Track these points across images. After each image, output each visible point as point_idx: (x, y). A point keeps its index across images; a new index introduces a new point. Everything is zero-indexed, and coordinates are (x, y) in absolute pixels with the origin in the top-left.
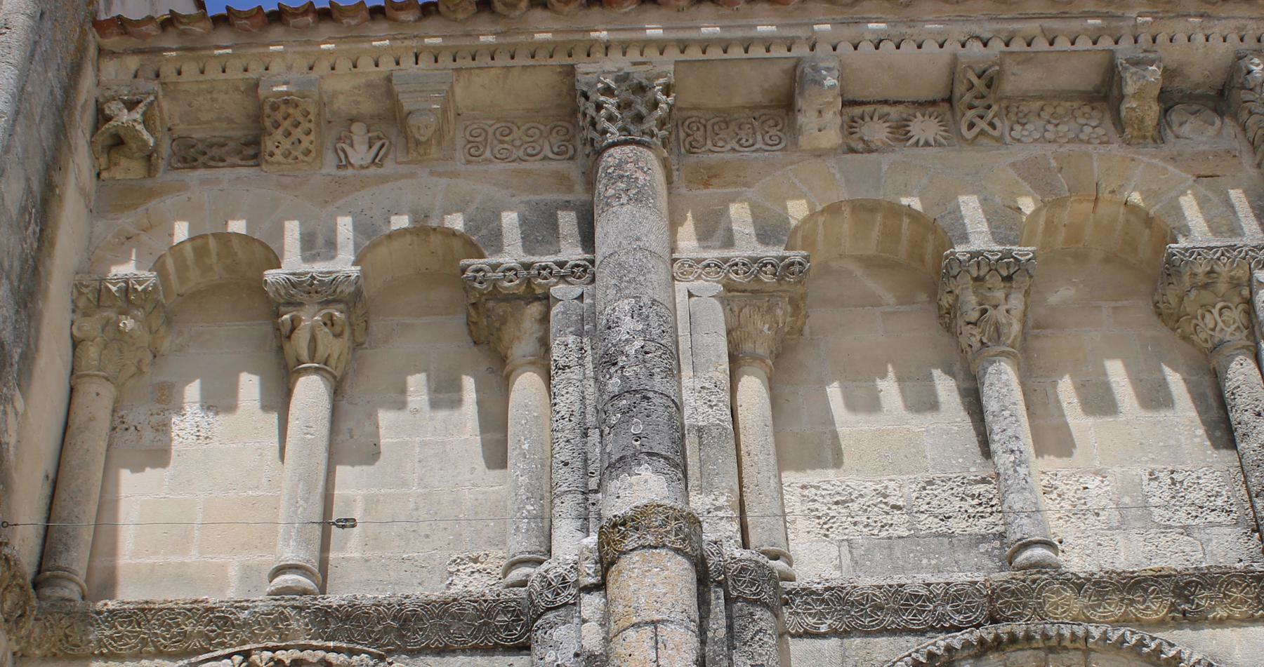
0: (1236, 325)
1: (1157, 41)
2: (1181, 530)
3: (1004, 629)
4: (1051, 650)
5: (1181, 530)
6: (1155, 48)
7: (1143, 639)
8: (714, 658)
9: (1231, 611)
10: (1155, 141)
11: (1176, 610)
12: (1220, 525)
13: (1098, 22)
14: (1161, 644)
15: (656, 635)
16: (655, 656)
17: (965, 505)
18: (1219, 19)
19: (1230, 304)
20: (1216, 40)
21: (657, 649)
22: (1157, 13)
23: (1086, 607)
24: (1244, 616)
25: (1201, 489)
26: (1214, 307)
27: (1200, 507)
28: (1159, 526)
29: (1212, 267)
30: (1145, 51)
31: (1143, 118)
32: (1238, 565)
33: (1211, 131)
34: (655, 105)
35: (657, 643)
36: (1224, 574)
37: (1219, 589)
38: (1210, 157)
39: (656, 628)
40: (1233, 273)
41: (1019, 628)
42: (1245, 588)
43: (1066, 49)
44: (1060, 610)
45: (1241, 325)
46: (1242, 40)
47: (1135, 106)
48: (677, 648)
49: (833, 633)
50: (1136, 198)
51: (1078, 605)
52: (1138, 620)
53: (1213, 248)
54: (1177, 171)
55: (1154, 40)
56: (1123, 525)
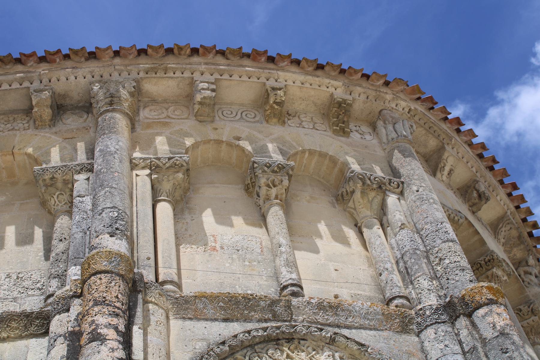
0: (65, 202)
1: (51, 81)
2: (12, 300)
5: (12, 300)
6: (50, 84)
9: (9, 333)
10: (50, 126)
12: (33, 295)
13: (22, 75)
18: (81, 68)
19: (63, 193)
20: (81, 79)
22: (52, 68)
24: (17, 335)
25: (31, 280)
26: (55, 195)
27: (27, 288)
29: (53, 176)
30: (45, 86)
31: (41, 116)
33: (81, 120)
36: (10, 315)
37: (5, 323)
38: (74, 131)
40: (64, 178)
42: (19, 321)
43: (7, 88)
45: (68, 202)
46: (93, 77)
47: (36, 110)
50: (30, 150)
53: (55, 167)
54: (56, 138)
55: (50, 81)
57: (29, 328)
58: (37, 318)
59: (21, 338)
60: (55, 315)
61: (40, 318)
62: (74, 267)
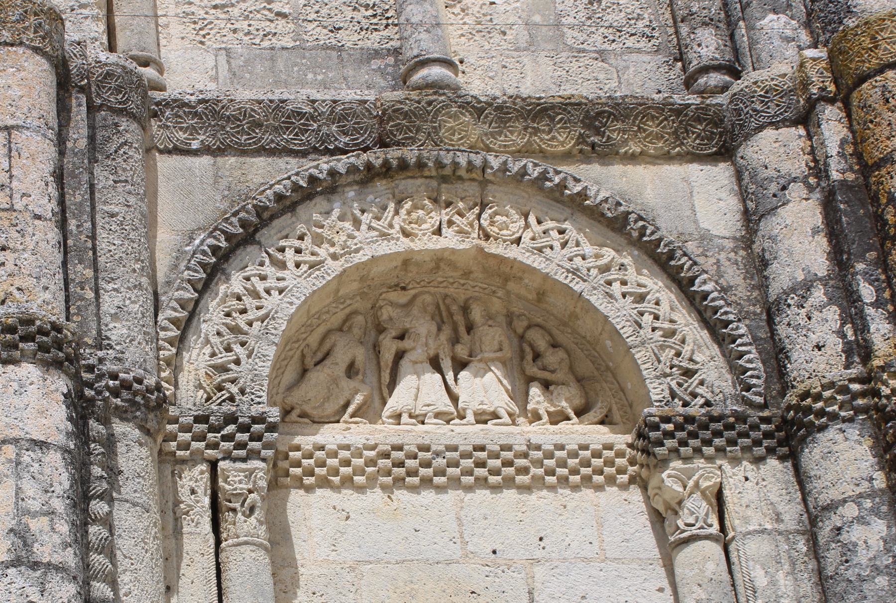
2: (596, 55)
3: (393, 154)
4: (444, 179)
5: (596, 55)
7: (546, 172)
8: (73, 171)
9: (645, 146)
11: (584, 142)
12: (639, 51)
14: (565, 178)
15: (10, 142)
16: (8, 165)
21: (10, 157)
23: (486, 135)
24: (659, 152)
25: (621, 11)
27: (618, 31)
28: (571, 49)
32: (656, 97)
35: (10, 150)
36: (641, 105)
37: (634, 122)
39: (10, 135)
41: (411, 154)
42: (662, 122)
44: (457, 136)
48: (32, 157)
49: (206, 150)
51: (476, 131)
52: (542, 151)
56: (531, 45)
57: (685, 139)
58: (699, 120)
59: (667, 158)
60: (760, 128)
61: (705, 120)
62: (771, 16)
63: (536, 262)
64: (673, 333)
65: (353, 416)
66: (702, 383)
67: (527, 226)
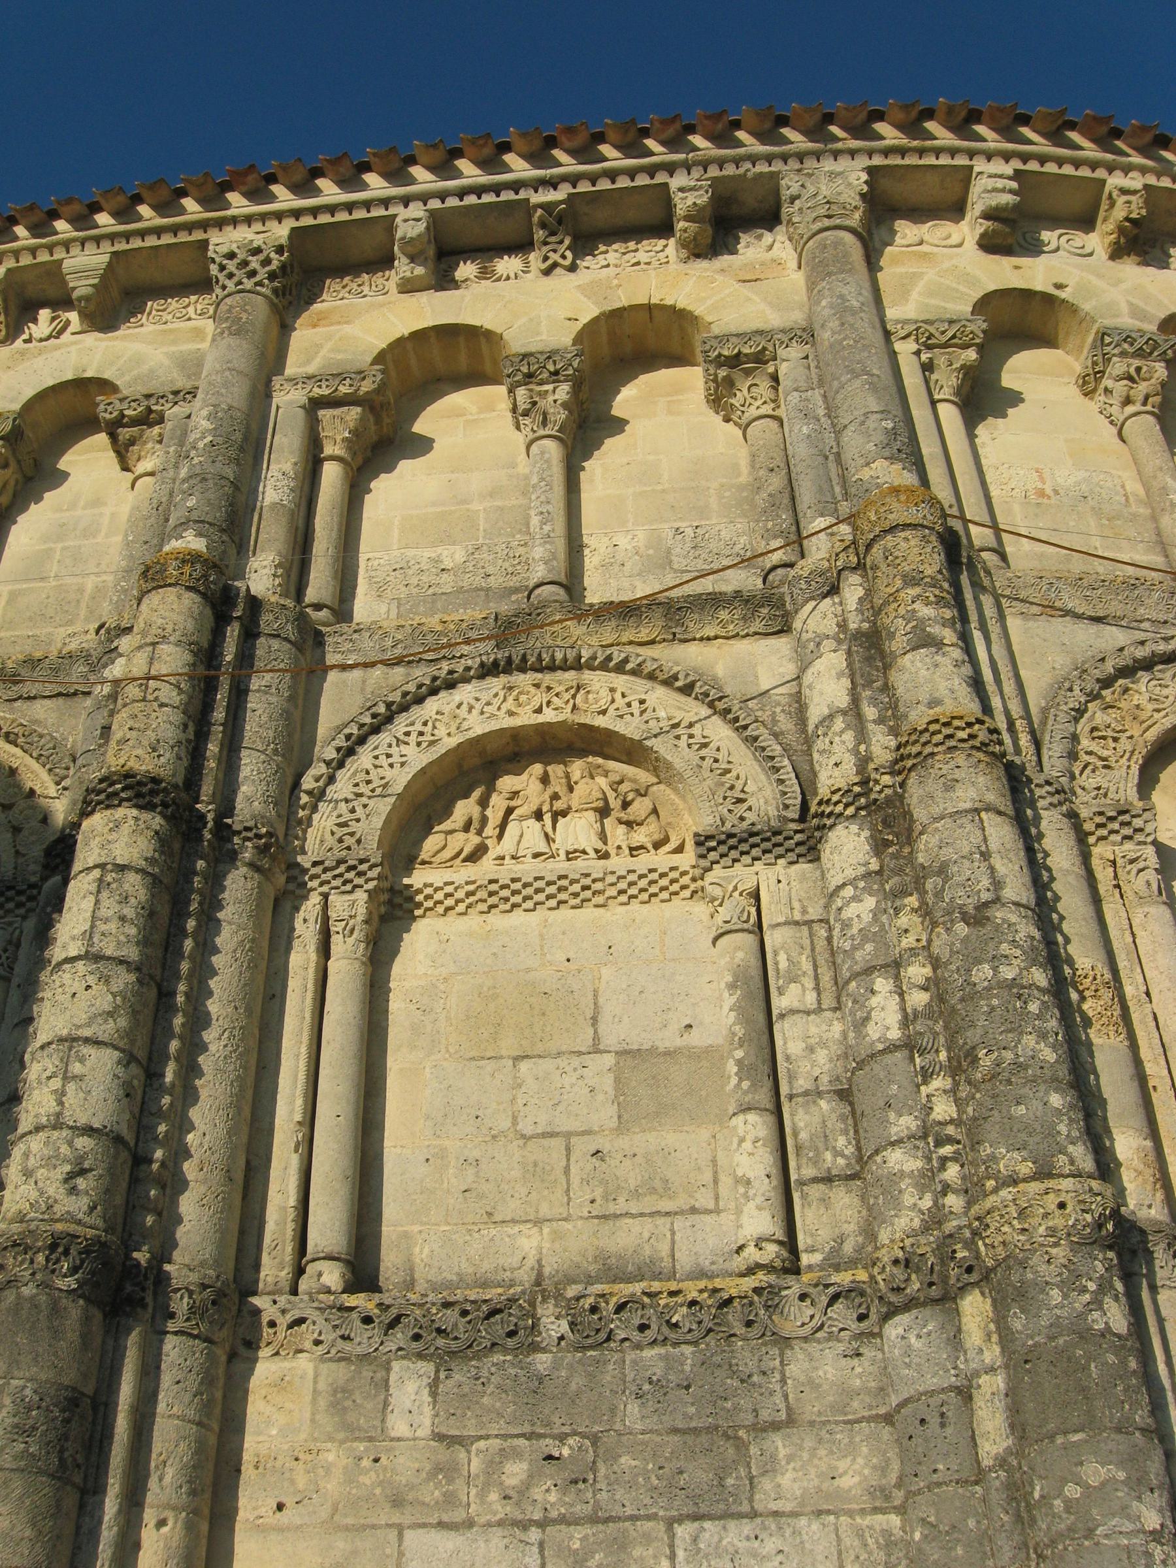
17: (506, 565)
34: (267, 262)
63: (619, 727)
64: (729, 771)
65: (464, 861)
66: (750, 809)
67: (613, 701)
